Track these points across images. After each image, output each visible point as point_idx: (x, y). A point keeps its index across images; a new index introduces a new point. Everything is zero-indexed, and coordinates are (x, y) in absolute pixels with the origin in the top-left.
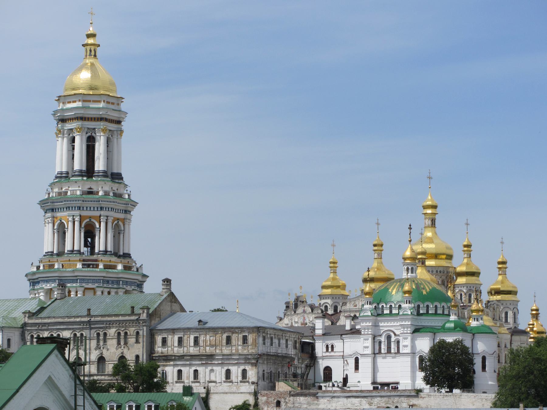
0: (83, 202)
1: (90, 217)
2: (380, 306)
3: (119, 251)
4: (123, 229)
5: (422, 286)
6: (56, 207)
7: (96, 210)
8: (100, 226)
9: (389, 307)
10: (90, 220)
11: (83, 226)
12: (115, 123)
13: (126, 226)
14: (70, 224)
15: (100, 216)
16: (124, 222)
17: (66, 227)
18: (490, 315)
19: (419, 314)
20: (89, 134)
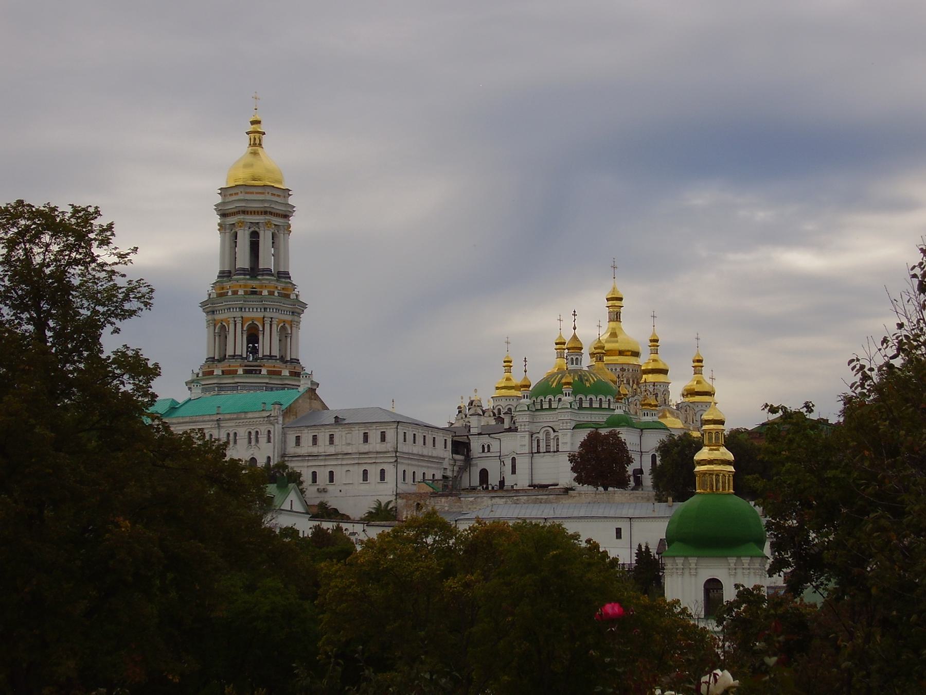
0: (244, 303)
1: (253, 319)
2: (539, 401)
3: (286, 356)
4: (290, 332)
5: (586, 378)
6: (216, 309)
7: (256, 310)
8: (264, 329)
9: (548, 400)
10: (253, 322)
11: (245, 329)
12: (282, 217)
13: (294, 329)
14: (232, 326)
15: (264, 318)
16: (291, 325)
17: (227, 330)
18: (680, 417)
19: (581, 408)
20: (252, 229)
